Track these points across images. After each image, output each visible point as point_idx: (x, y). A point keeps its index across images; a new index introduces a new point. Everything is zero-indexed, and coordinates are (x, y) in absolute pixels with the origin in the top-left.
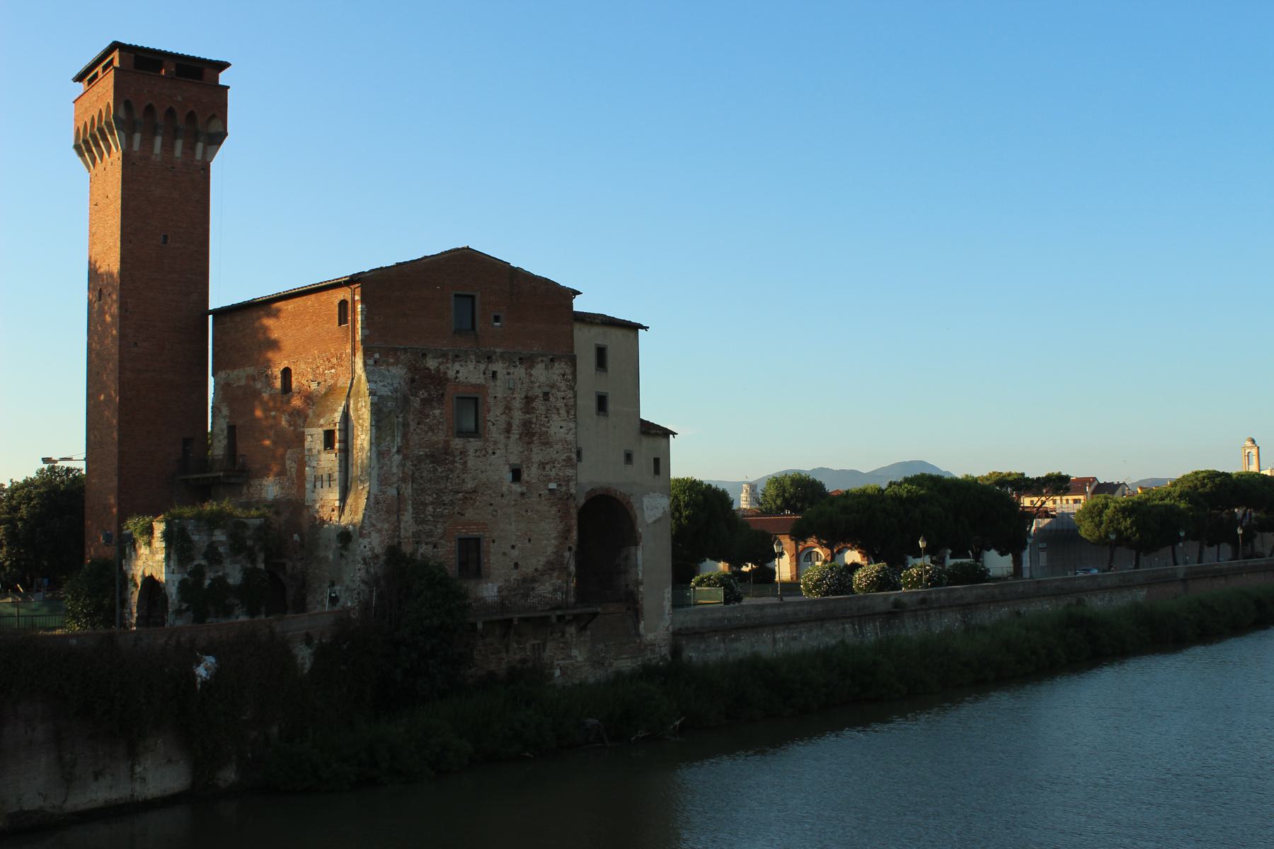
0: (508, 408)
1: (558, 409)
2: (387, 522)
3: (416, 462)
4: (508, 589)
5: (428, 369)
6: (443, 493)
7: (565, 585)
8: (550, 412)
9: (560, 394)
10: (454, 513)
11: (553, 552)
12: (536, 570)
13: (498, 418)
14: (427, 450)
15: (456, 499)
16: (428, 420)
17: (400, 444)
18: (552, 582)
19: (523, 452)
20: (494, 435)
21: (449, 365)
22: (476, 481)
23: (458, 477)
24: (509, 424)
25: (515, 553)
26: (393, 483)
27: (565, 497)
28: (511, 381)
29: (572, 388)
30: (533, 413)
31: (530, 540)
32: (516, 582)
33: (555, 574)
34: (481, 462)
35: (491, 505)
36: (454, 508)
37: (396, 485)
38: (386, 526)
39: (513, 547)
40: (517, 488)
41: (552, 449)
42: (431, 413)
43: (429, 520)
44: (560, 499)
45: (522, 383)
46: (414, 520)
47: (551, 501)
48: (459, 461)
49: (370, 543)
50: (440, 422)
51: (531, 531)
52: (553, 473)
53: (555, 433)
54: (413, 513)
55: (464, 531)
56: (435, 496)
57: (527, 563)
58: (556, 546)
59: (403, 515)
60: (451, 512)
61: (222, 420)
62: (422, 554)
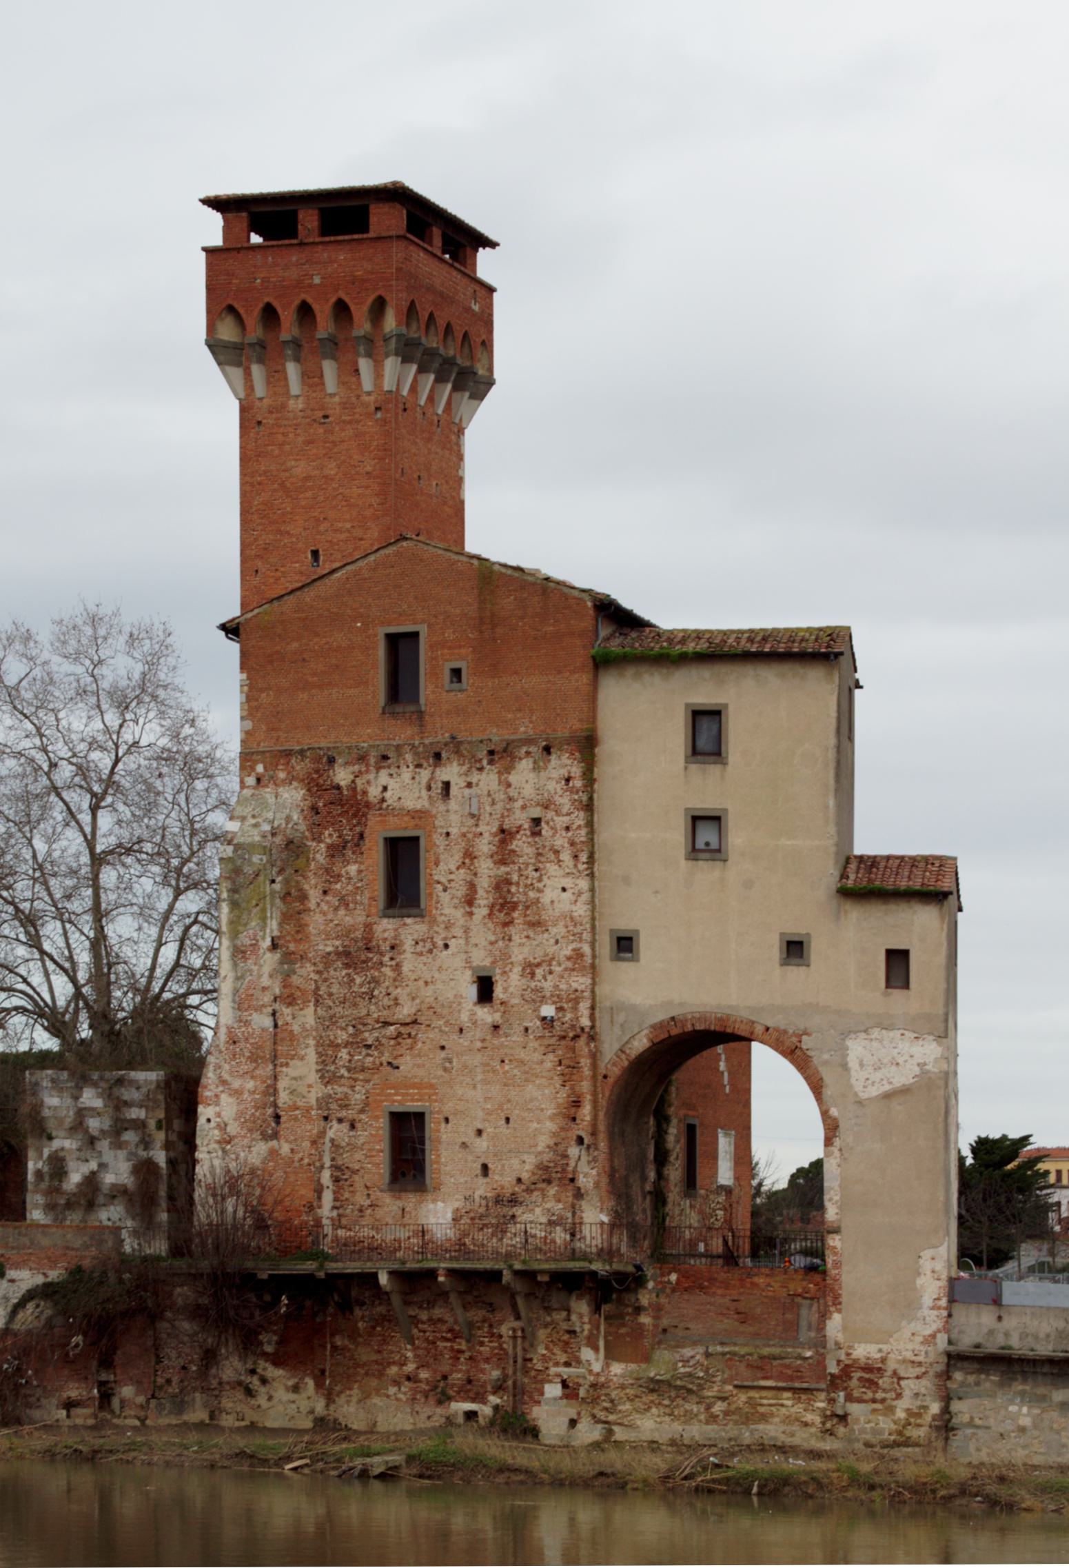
0: (469, 856)
1: (557, 852)
2: (252, 1077)
3: (321, 967)
4: (472, 1215)
5: (338, 787)
6: (365, 1025)
7: (569, 1215)
8: (543, 859)
9: (561, 821)
10: (381, 1064)
11: (548, 1147)
12: (519, 1180)
13: (452, 877)
14: (338, 943)
15: (383, 1037)
16: (338, 886)
17: (276, 933)
18: (548, 1205)
19: (496, 942)
20: (446, 911)
21: (371, 776)
22: (418, 1001)
23: (389, 994)
24: (472, 887)
25: (482, 1144)
26: (263, 1006)
27: (571, 1035)
28: (474, 801)
29: (589, 807)
30: (513, 863)
31: (508, 1120)
32: (484, 1202)
33: (552, 1190)
34: (425, 964)
35: (443, 1048)
36: (382, 1053)
37: (270, 1010)
38: (250, 1085)
39: (479, 1132)
40: (486, 1015)
41: (546, 935)
42: (343, 872)
43: (342, 1076)
44: (564, 1038)
45: (493, 803)
46: (320, 1074)
47: (546, 1042)
48: (389, 963)
49: (218, 1115)
50: (358, 888)
51: (509, 1101)
52: (548, 985)
53: (552, 902)
54: (317, 1063)
55: (399, 1098)
56: (351, 1030)
57: (503, 1166)
58: (554, 1134)
59: (287, 1065)
60: (377, 1063)
62: (332, 1140)
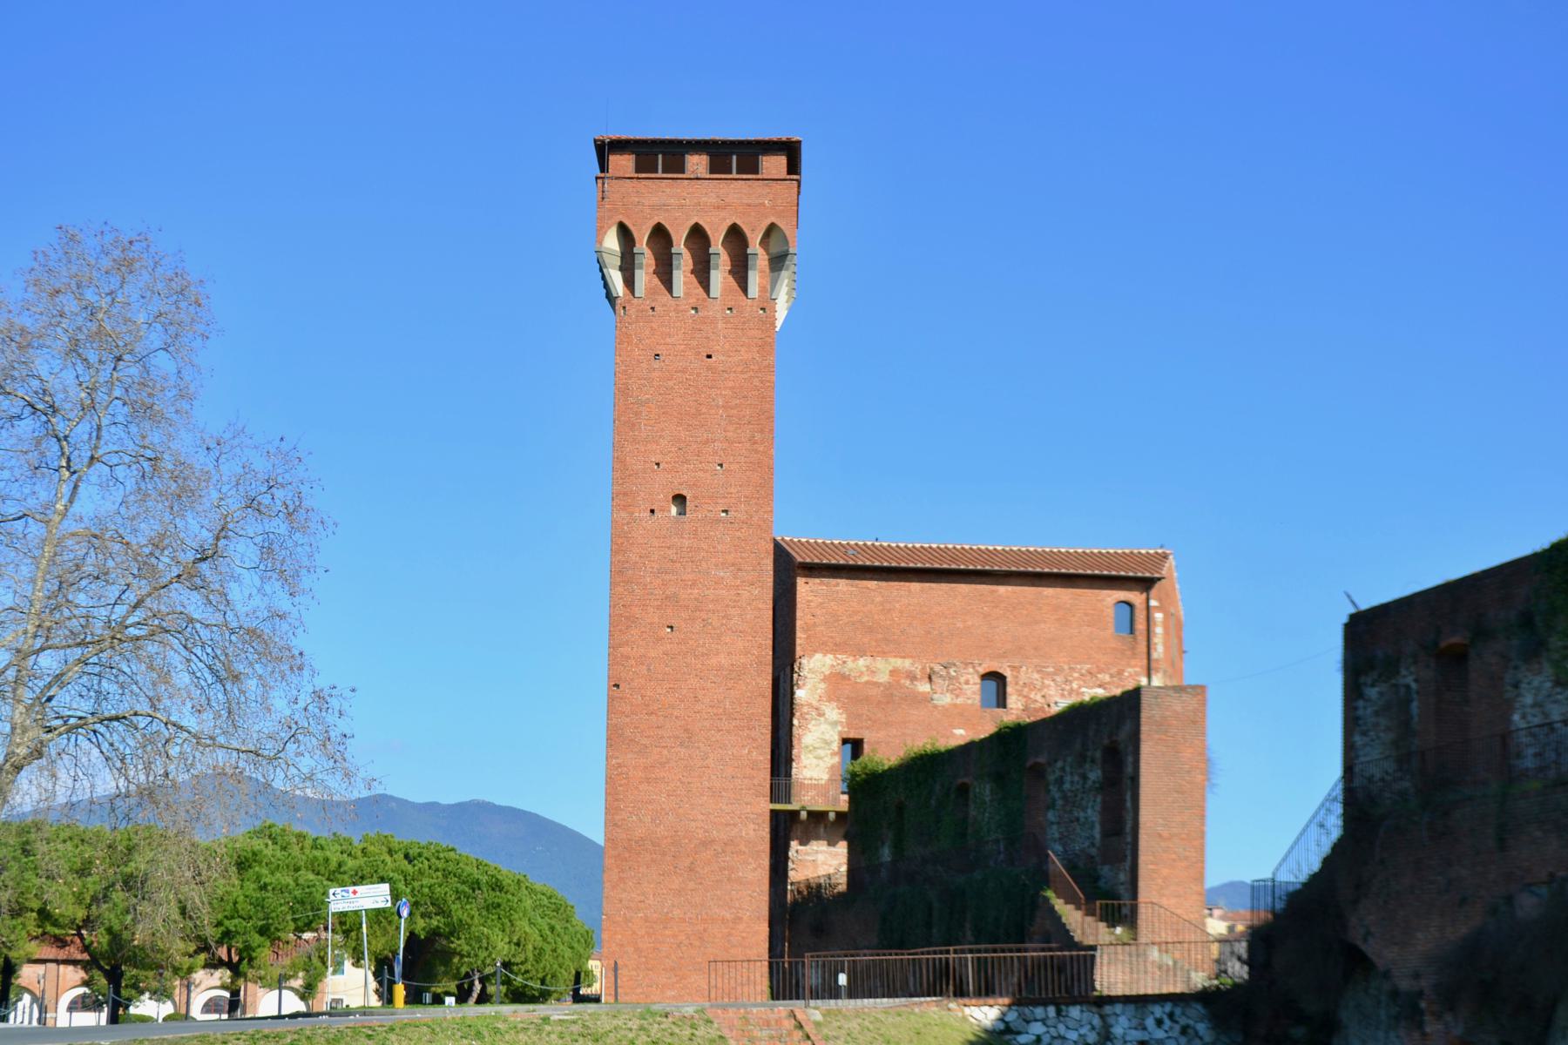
61: (824, 727)
